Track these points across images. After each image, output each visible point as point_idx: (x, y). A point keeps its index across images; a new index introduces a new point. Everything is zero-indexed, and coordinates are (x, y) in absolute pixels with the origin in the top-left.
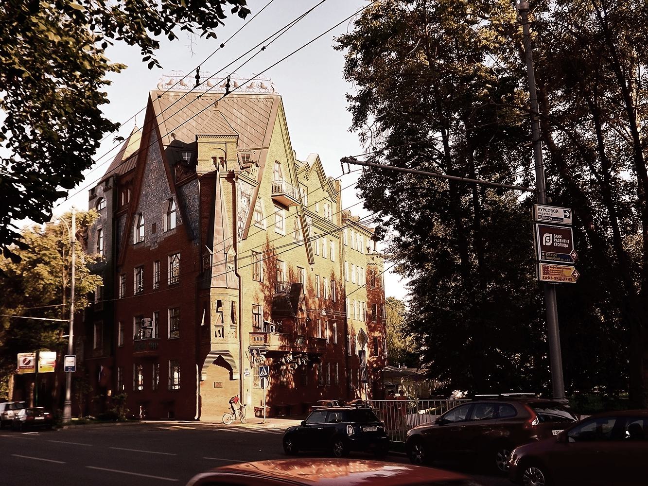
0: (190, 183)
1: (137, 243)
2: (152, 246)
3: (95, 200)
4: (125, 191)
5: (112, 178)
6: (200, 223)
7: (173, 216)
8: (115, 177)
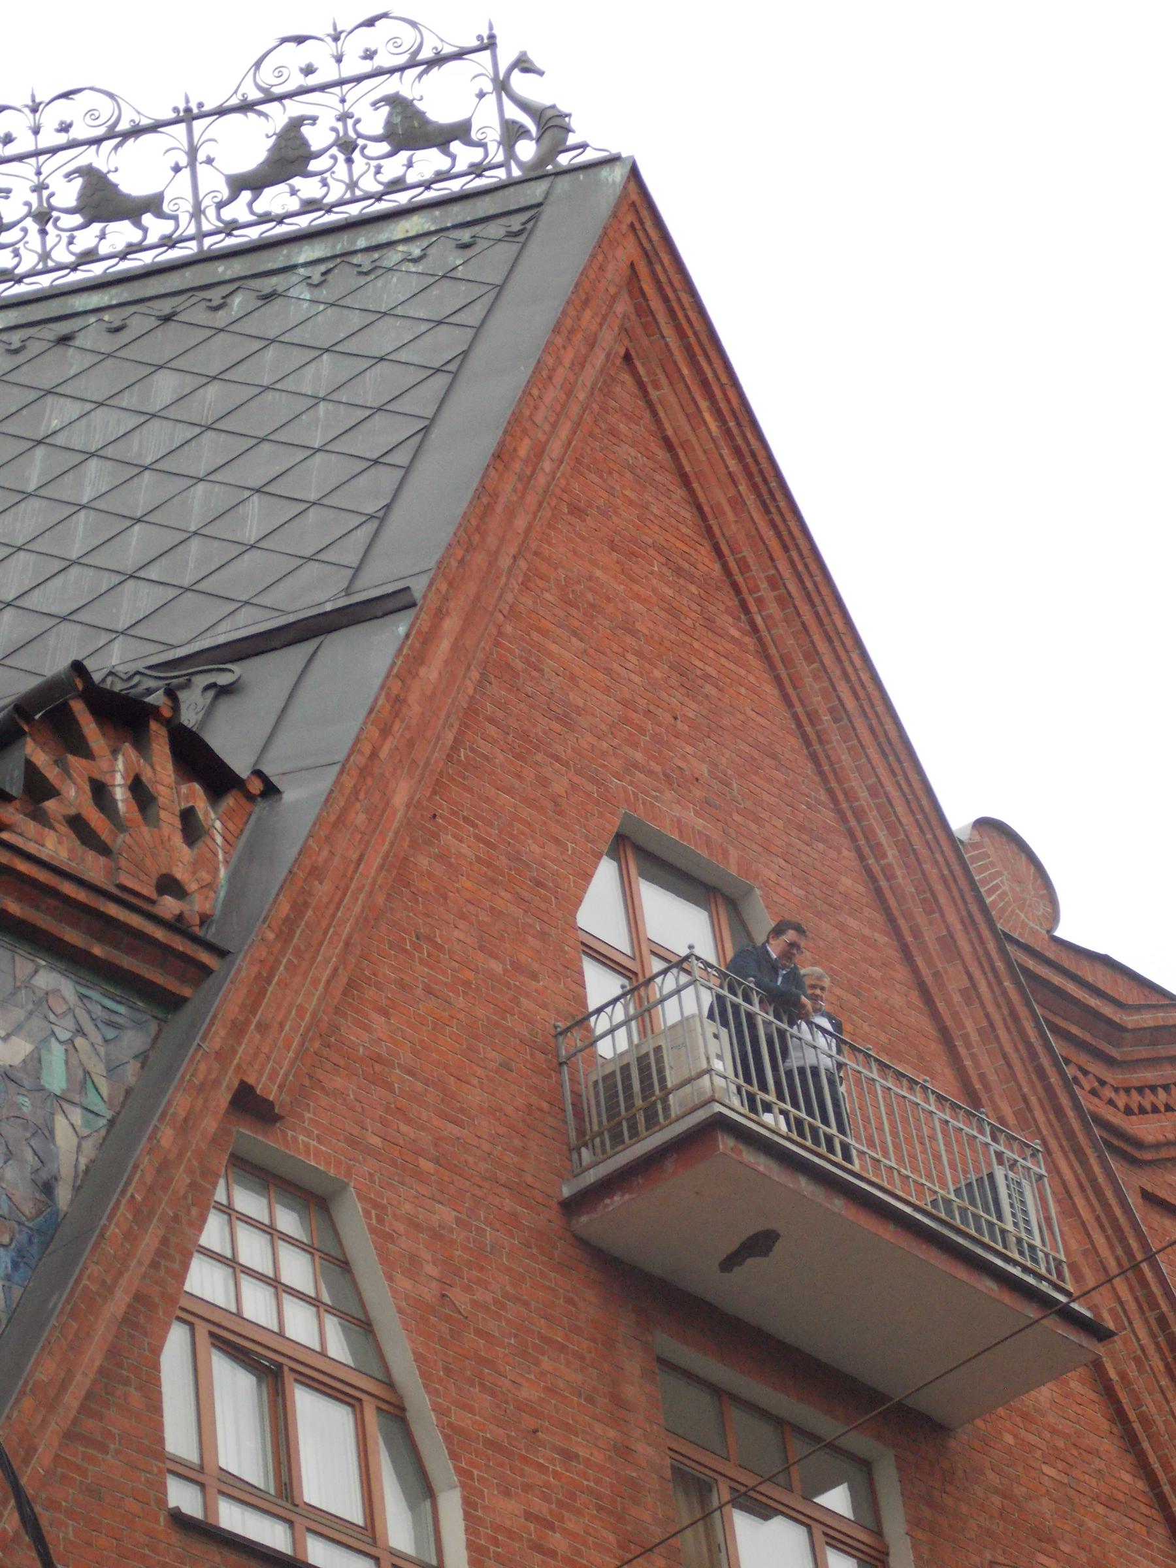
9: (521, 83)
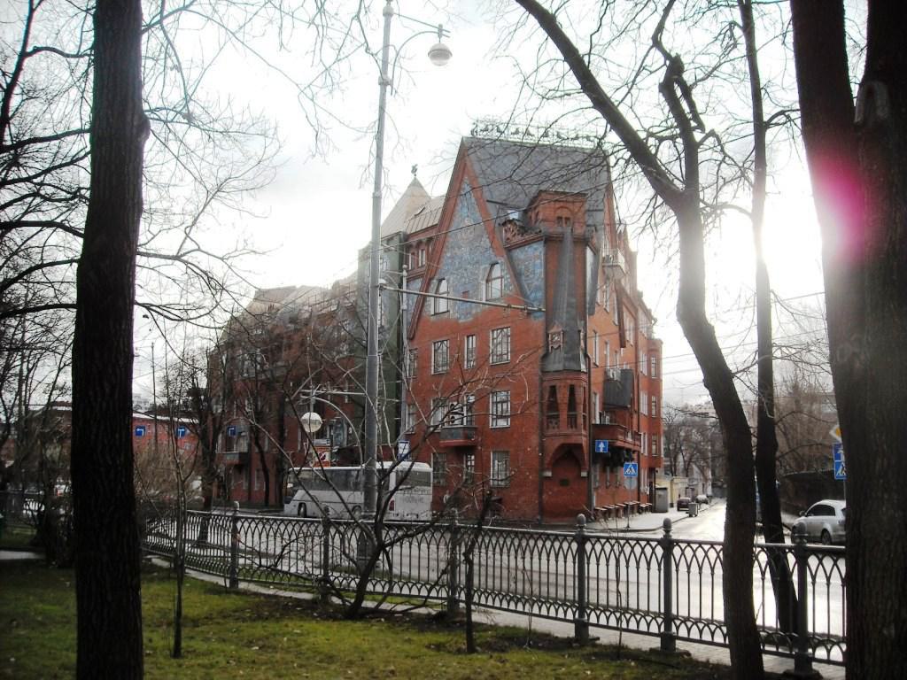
1: (435, 314)
2: (463, 317)
5: (398, 237)
6: (546, 292)
7: (496, 284)
8: (402, 236)
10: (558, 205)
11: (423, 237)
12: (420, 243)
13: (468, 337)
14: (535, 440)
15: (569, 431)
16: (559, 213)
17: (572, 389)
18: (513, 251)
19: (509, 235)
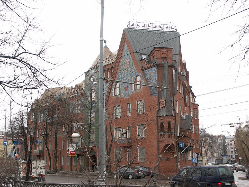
0: (150, 69)
1: (115, 96)
3: (89, 77)
4: (107, 72)
9: (176, 27)
10: (162, 53)
11: (110, 67)
12: (108, 69)
13: (128, 104)
14: (155, 143)
15: (169, 139)
16: (162, 56)
17: (169, 123)
18: (145, 70)
19: (143, 65)
